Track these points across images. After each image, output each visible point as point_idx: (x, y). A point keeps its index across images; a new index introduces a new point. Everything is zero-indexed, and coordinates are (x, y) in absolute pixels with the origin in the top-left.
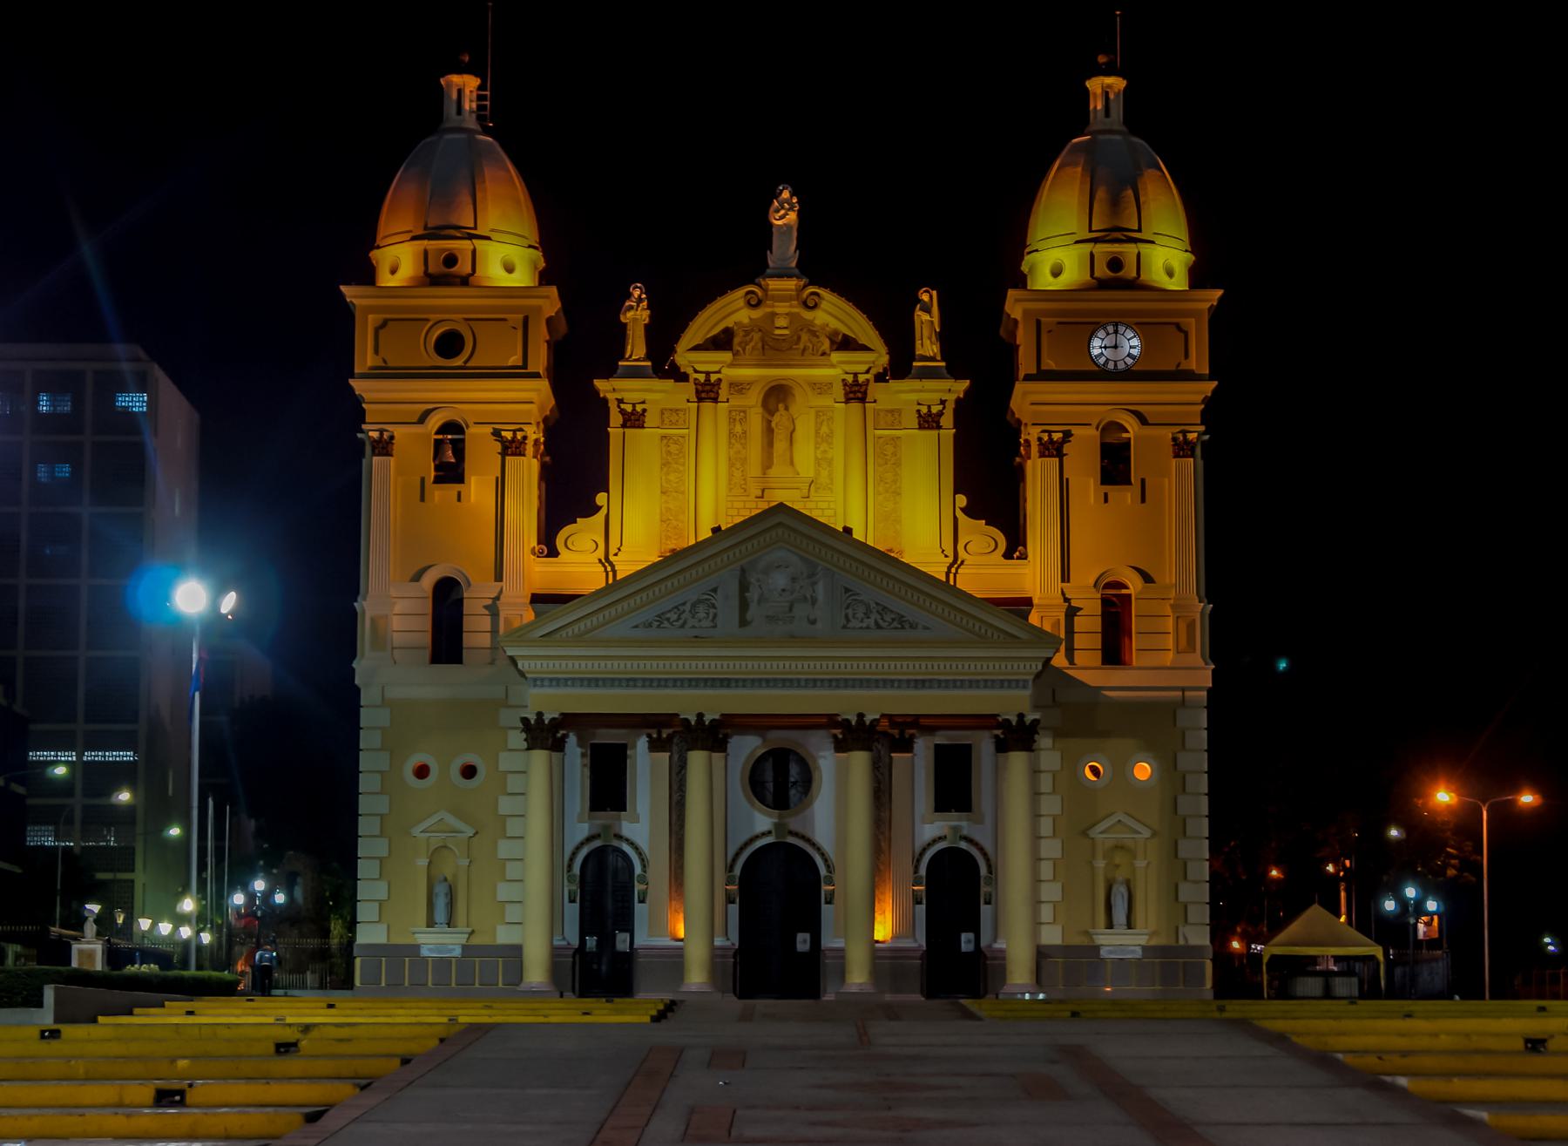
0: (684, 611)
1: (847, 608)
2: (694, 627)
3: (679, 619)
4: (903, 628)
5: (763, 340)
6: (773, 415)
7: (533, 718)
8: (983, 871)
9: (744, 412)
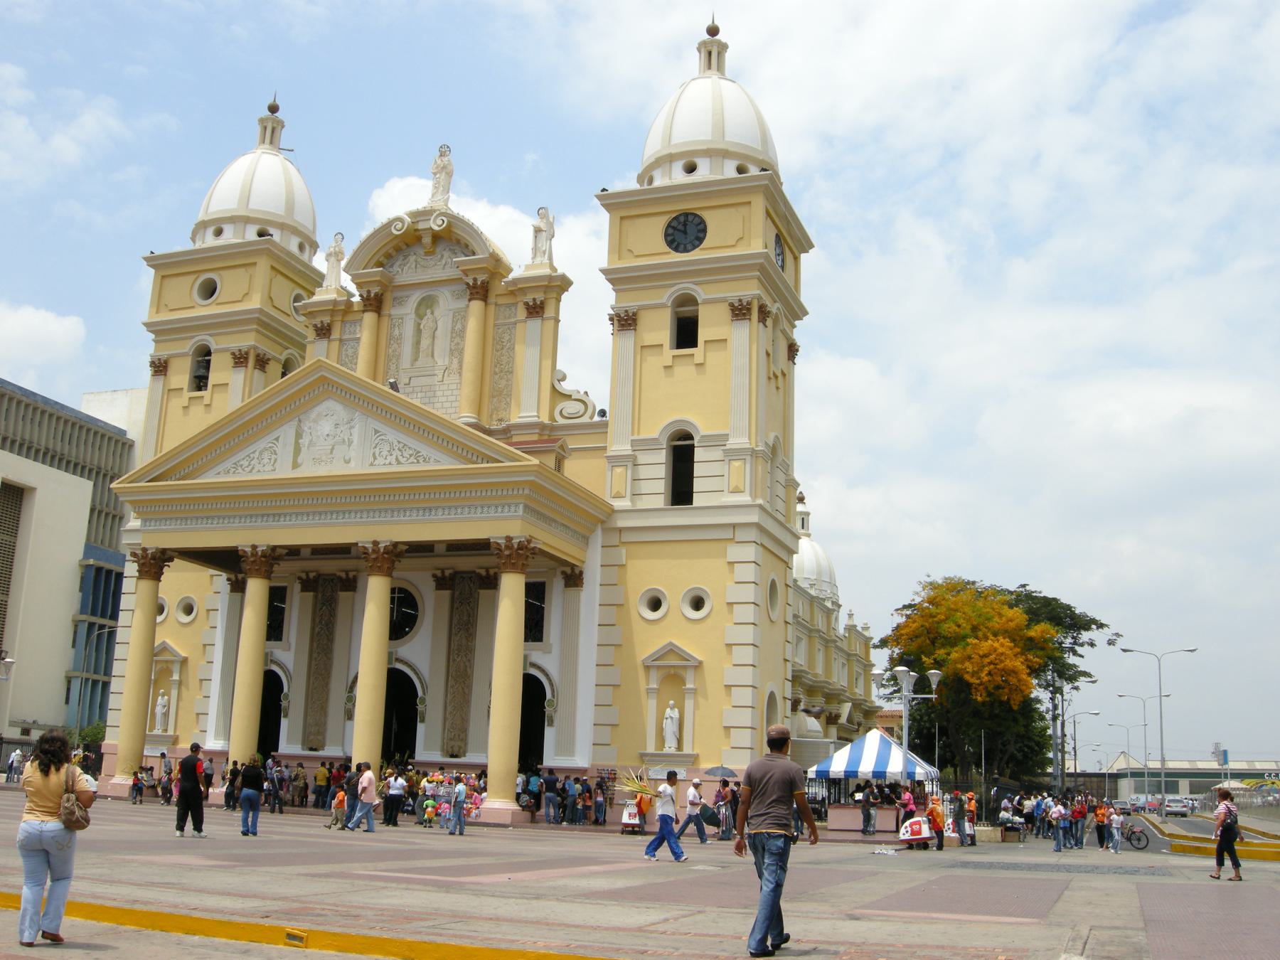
0: (254, 458)
1: (375, 447)
2: (259, 471)
4: (418, 462)
5: (416, 261)
8: (549, 695)
9: (402, 319)
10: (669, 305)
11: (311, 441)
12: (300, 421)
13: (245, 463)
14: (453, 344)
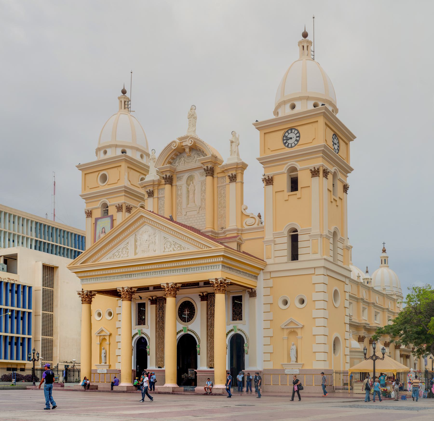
1: (165, 244)
2: (122, 257)
3: (118, 255)
4: (181, 250)
6: (189, 186)
9: (181, 186)
10: (286, 172)
11: (141, 243)
12: (136, 235)
13: (117, 254)
14: (202, 196)
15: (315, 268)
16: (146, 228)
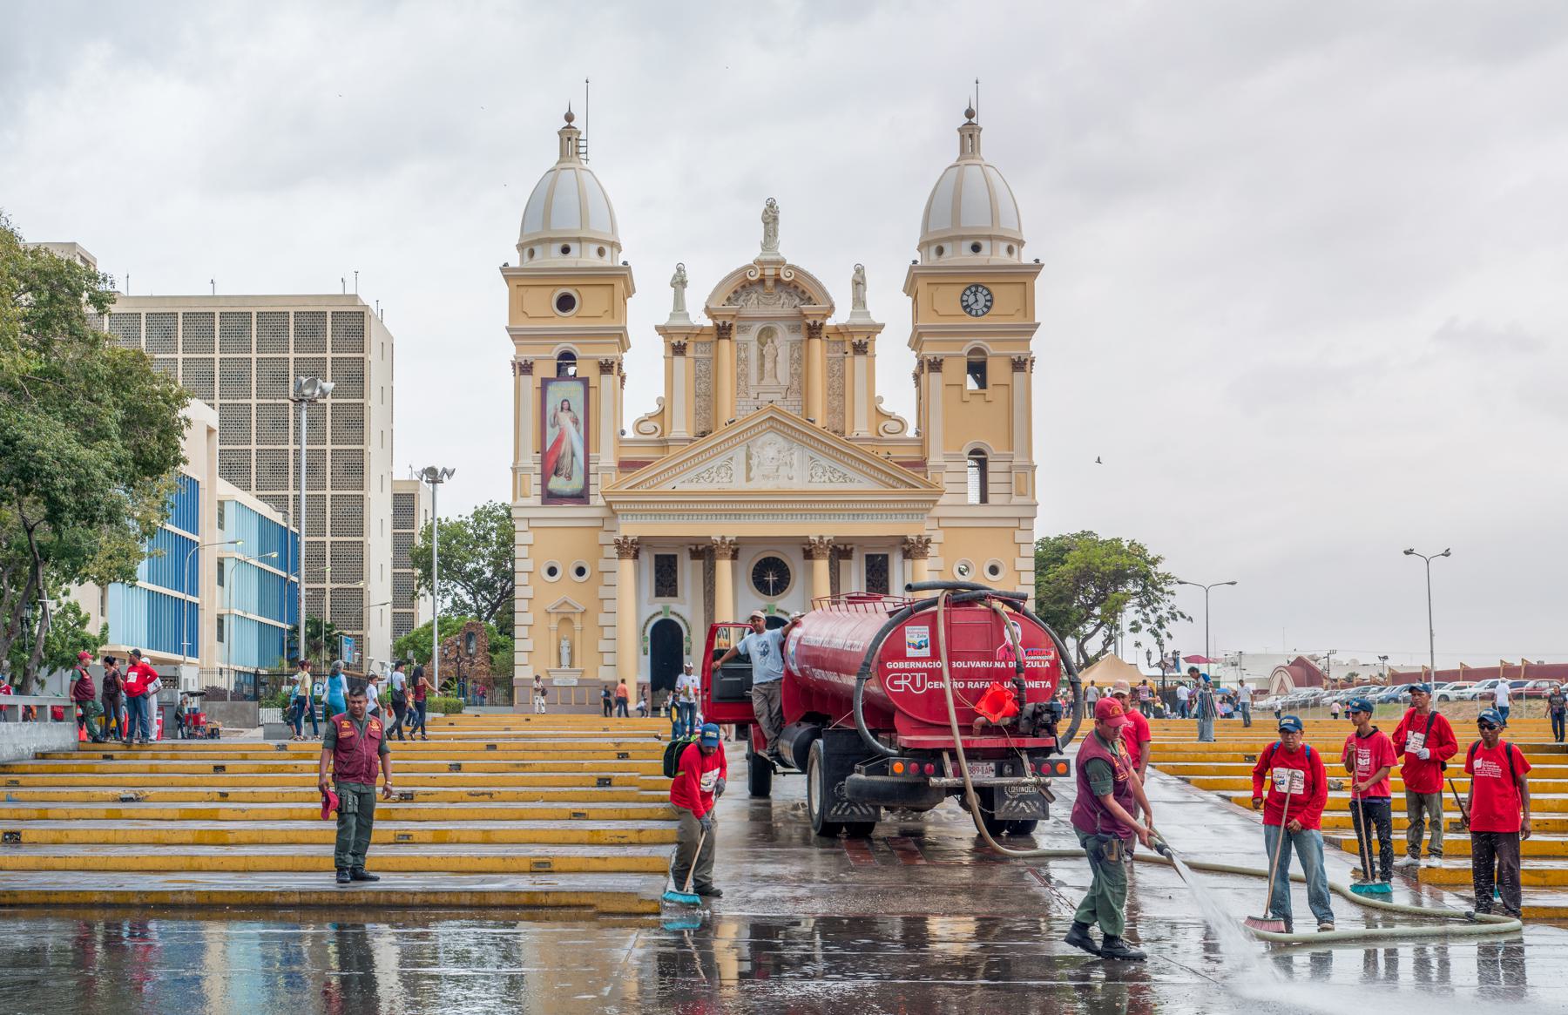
6: (764, 346)
7: (621, 539)
15: (1019, 518)
16: (770, 436)
